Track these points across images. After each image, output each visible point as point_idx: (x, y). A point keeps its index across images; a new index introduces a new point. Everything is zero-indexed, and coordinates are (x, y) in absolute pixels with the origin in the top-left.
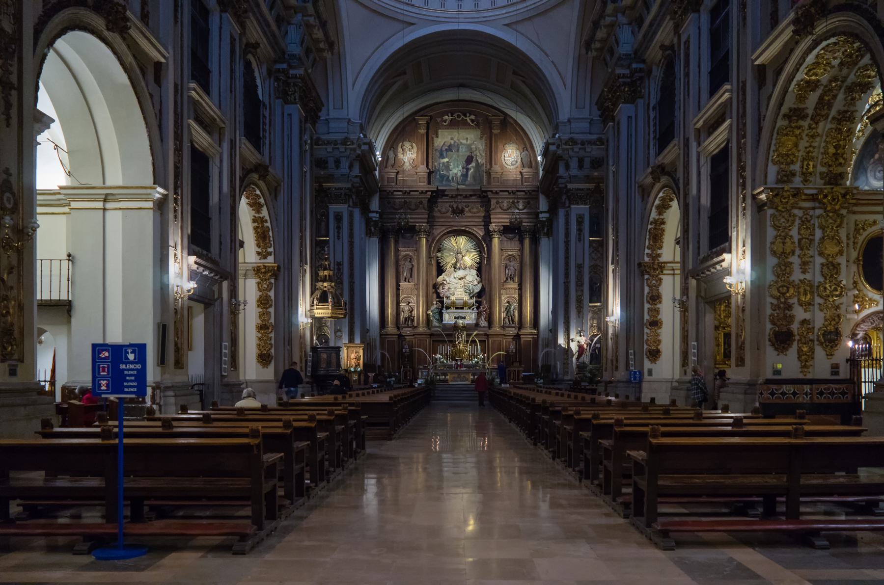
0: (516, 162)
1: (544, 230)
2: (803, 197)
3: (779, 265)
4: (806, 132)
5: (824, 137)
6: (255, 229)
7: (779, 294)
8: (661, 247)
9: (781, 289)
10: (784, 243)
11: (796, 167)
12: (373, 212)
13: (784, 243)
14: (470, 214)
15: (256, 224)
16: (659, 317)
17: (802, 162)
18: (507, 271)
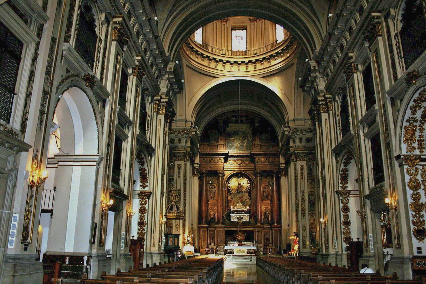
1: (283, 173)
12: (196, 164)
16: (349, 220)
18: (264, 194)
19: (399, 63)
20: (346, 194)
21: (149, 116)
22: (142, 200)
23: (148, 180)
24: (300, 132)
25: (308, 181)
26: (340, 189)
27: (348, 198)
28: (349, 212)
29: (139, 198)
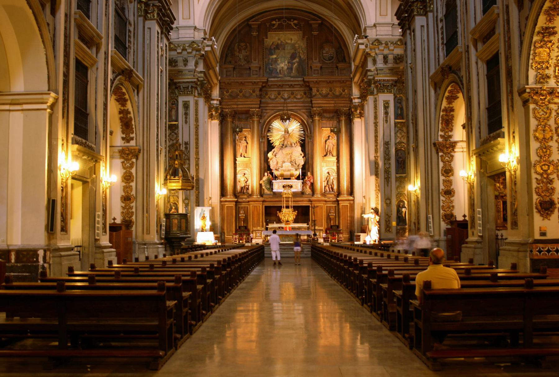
0: (333, 57)
3: (541, 148)
7: (542, 171)
8: (452, 130)
9: (543, 167)
10: (544, 131)
13: (544, 131)
14: (295, 100)
16: (452, 187)
24: (384, 45)
25: (395, 126)
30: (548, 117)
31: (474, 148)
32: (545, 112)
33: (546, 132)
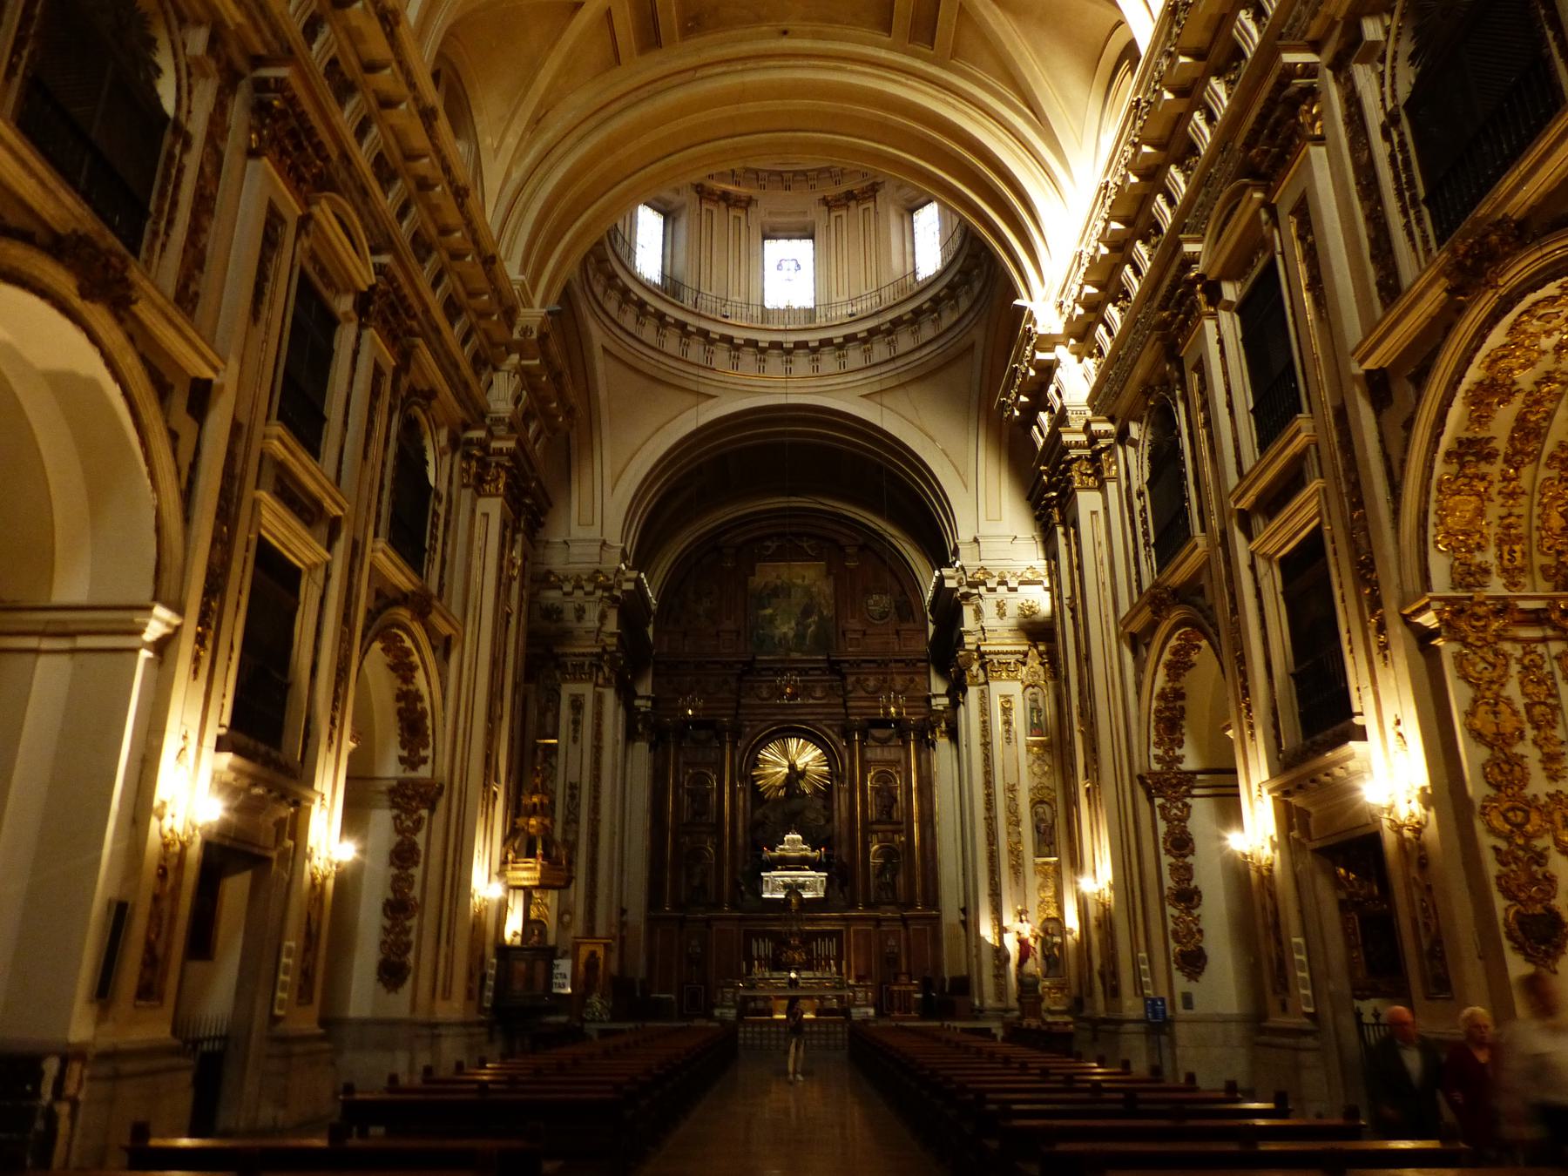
2: (1517, 616)
4: (1497, 486)
5: (1537, 497)
6: (400, 712)
7: (1508, 827)
9: (1510, 814)
11: (1490, 557)
13: (1496, 713)
15: (402, 704)
16: (1193, 884)
17: (1500, 545)
19: (1407, 226)
20: (1180, 784)
21: (439, 498)
22: (403, 816)
23: (431, 740)
26: (1156, 767)
27: (1188, 800)
28: (1192, 852)
29: (394, 805)
30: (1501, 677)
31: (1265, 776)
32: (1490, 664)
33: (1502, 717)
